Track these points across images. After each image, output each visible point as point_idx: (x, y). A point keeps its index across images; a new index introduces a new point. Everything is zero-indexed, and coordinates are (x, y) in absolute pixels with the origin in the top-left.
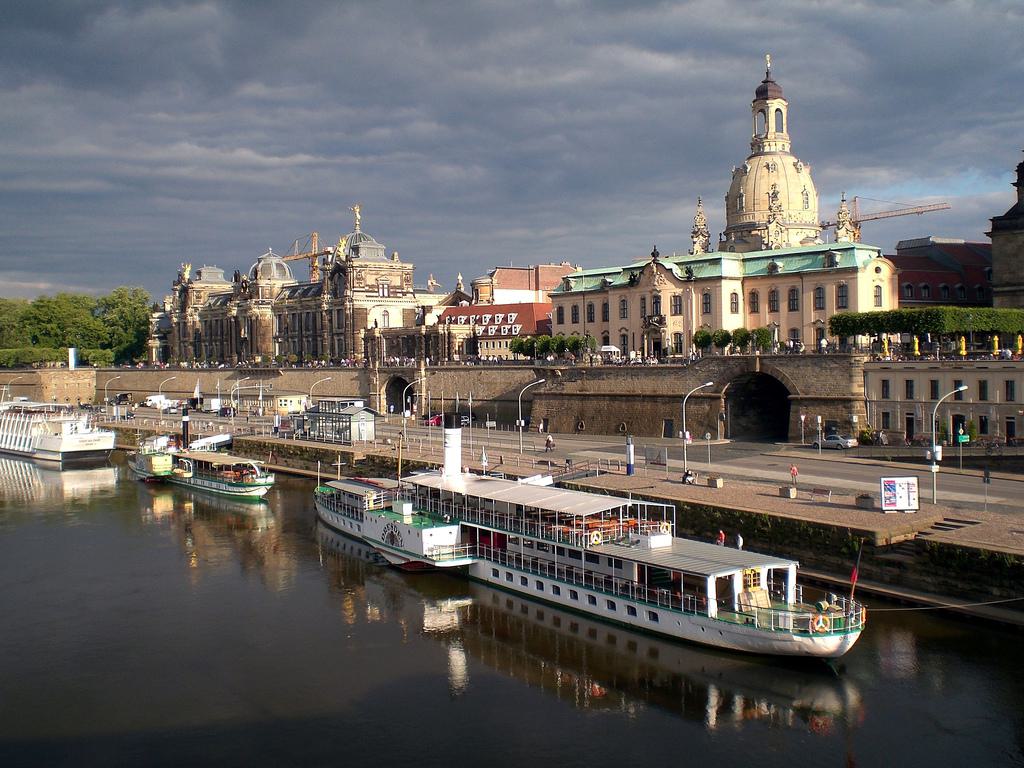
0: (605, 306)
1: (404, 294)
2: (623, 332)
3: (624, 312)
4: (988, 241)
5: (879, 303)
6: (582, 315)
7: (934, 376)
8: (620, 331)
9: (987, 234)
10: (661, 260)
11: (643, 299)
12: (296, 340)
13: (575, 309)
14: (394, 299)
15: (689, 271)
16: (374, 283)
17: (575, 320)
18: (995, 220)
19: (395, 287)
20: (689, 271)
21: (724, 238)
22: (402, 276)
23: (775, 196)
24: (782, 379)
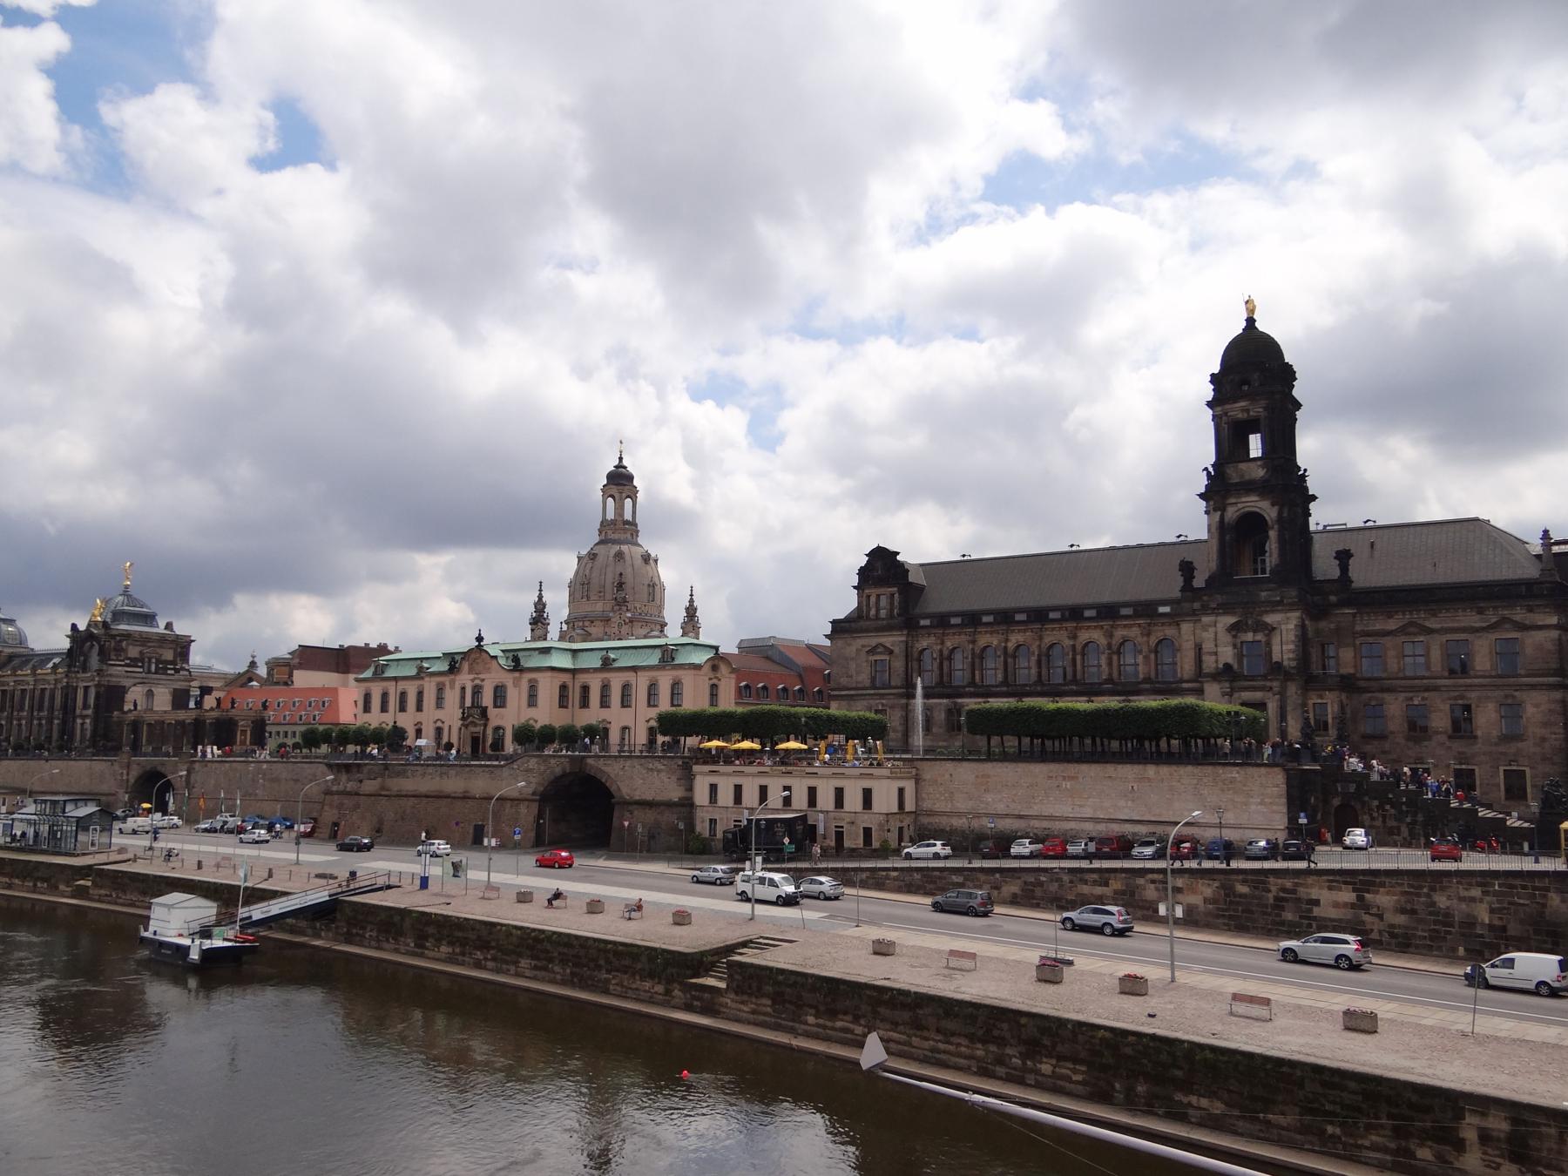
1: (177, 671)
4: (828, 643)
7: (764, 781)
11: (463, 689)
13: (385, 696)
17: (384, 709)
18: (834, 622)
20: (516, 660)
21: (565, 627)
23: (620, 586)
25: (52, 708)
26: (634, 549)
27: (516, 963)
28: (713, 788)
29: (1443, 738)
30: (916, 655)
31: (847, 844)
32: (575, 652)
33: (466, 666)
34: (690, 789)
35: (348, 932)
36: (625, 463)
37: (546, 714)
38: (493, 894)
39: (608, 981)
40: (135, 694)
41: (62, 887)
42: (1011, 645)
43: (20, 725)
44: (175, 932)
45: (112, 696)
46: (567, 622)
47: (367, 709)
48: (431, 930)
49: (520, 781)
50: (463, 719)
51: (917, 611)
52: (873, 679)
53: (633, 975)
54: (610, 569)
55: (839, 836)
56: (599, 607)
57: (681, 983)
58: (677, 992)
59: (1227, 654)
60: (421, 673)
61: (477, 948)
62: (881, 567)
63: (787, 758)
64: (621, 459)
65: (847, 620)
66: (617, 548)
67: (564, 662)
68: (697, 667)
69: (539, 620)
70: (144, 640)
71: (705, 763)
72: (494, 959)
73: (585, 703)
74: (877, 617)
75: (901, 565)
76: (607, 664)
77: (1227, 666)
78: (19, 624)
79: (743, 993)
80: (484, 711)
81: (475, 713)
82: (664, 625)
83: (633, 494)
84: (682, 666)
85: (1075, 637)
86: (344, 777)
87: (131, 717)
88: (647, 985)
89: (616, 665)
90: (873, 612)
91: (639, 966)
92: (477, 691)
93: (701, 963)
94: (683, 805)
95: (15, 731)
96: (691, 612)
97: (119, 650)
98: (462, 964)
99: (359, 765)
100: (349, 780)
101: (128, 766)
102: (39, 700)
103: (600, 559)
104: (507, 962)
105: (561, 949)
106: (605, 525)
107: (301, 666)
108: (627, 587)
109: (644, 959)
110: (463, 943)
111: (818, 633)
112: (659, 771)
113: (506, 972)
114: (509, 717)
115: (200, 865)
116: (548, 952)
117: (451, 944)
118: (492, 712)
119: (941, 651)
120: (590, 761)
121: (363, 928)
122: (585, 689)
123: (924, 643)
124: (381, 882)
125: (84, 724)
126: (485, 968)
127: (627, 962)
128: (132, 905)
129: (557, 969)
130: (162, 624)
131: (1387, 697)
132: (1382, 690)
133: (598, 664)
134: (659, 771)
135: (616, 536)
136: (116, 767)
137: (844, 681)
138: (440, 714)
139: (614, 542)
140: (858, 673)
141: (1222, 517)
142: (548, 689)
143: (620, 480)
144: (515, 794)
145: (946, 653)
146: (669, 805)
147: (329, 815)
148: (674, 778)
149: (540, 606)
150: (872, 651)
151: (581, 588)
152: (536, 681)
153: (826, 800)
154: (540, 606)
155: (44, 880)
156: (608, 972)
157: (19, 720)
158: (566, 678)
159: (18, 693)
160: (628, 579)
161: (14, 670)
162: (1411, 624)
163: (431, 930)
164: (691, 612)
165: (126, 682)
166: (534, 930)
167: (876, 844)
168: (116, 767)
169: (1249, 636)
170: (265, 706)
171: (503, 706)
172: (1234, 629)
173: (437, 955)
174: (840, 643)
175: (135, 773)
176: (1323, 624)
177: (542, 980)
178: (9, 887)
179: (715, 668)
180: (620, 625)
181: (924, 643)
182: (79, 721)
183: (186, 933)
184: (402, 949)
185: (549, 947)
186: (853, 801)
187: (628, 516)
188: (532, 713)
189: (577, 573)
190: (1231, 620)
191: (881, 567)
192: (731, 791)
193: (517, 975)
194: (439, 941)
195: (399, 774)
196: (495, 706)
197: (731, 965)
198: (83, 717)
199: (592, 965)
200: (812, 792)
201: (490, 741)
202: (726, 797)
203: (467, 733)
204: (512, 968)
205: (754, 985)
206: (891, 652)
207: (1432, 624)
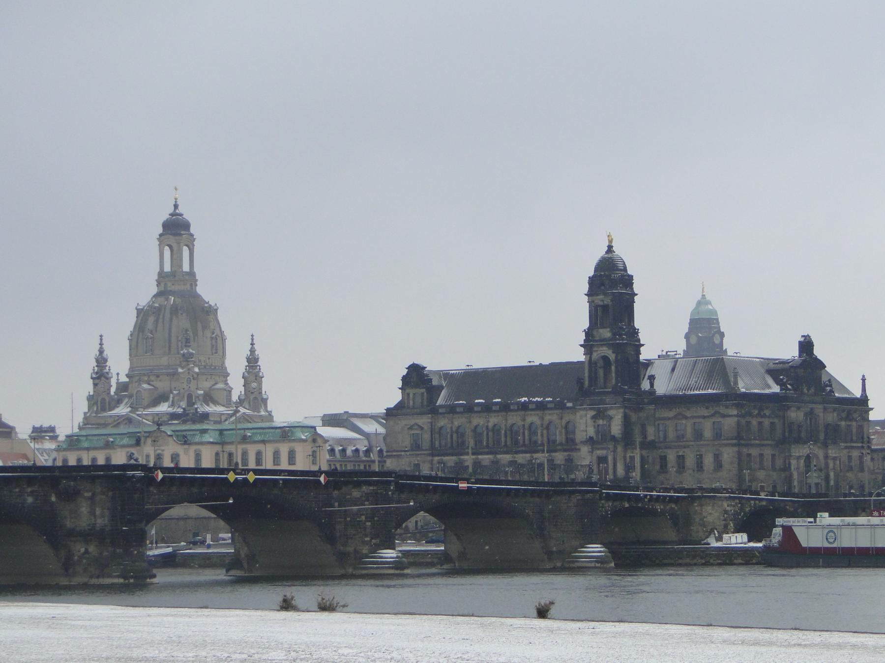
29: (691, 471)
30: (437, 430)
33: (149, 441)
36: (180, 210)
42: (491, 425)
46: (127, 376)
56: (164, 361)
59: (591, 432)
64: (176, 206)
77: (591, 438)
85: (524, 420)
90: (411, 403)
96: (253, 361)
131: (669, 451)
132: (666, 448)
141: (590, 357)
149: (101, 361)
150: (411, 428)
152: (200, 451)
154: (101, 361)
162: (679, 414)
164: (253, 361)
169: (601, 422)
172: (594, 418)
176: (641, 414)
180: (189, 381)
187: (186, 268)
190: (593, 413)
206: (422, 428)
207: (688, 414)
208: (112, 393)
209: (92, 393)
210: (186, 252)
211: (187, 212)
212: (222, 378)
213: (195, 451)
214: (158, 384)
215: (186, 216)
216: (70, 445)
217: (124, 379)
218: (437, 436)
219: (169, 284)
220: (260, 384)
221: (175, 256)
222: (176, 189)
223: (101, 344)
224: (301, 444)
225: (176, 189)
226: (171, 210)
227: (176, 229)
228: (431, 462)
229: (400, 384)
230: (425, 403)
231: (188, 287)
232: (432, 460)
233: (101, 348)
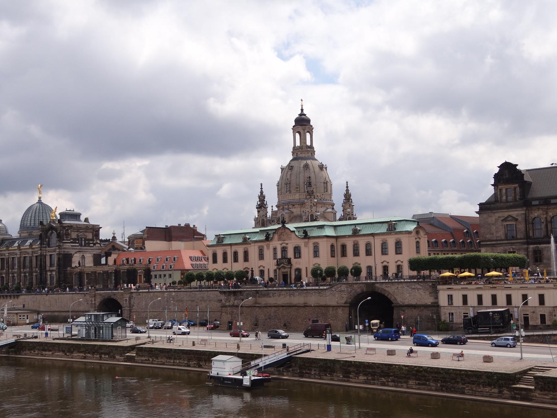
0: (246, 254)
1: (94, 244)
2: (262, 268)
3: (261, 256)
4: (478, 216)
5: (418, 251)
6: (230, 257)
7: (480, 292)
8: (259, 267)
9: (477, 212)
10: (287, 226)
11: (275, 249)
12: (27, 274)
13: (225, 255)
14: (89, 248)
15: (305, 232)
16: (76, 237)
17: (225, 260)
18: (480, 205)
19: (89, 240)
20: (305, 232)
21: (275, 209)
22: (93, 233)
23: (310, 184)
24: (388, 295)
25: (31, 267)
26: (313, 162)
27: (407, 383)
28: (450, 297)
30: (531, 221)
31: (531, 323)
32: (335, 227)
33: (276, 237)
34: (437, 298)
35: (300, 372)
36: (305, 112)
37: (325, 261)
38: (371, 352)
39: (464, 388)
40: (76, 260)
41: (117, 357)
43: (13, 277)
44: (227, 373)
45: (66, 259)
46: (277, 206)
47: (215, 261)
48: (352, 369)
49: (336, 296)
50: (278, 265)
51: (529, 196)
52: (506, 235)
53: (479, 385)
54: (302, 175)
55: (526, 319)
56: (297, 196)
57: (507, 388)
58: (505, 392)
60: (245, 241)
61: (381, 376)
62: (508, 174)
63: (490, 280)
64: (302, 110)
65: (488, 203)
66: (305, 162)
67: (330, 232)
68: (409, 232)
69: (262, 206)
70: (78, 228)
71: (444, 284)
72: (393, 381)
73: (344, 254)
74: (507, 201)
75: (519, 172)
76: (356, 233)
78: (3, 222)
79: (545, 390)
80: (289, 260)
81: (284, 261)
82: (333, 205)
83: (311, 132)
84: (401, 233)
86: (232, 298)
87: (78, 270)
88: (487, 389)
89: (361, 233)
90: (504, 198)
91: (482, 381)
92: (284, 250)
93: (515, 378)
94: (434, 306)
95: (11, 280)
96: (348, 197)
97: (68, 235)
98: (374, 384)
99: (241, 291)
100: (235, 299)
101: (95, 296)
102: (23, 264)
103: (295, 169)
104: (401, 382)
105: (434, 375)
106: (295, 149)
107: (148, 239)
108: (312, 184)
109: (484, 377)
110: (373, 374)
111: (470, 210)
112: (420, 289)
113: (402, 387)
114: (306, 263)
115: (194, 344)
116: (426, 377)
117: (365, 375)
118: (294, 261)
119: (546, 218)
120: (377, 285)
121: (311, 370)
122: (344, 247)
123: (536, 214)
124: (304, 349)
125: (52, 273)
126: (388, 386)
127: (474, 379)
128: (163, 364)
129: (432, 384)
130: (82, 218)
133: (350, 233)
134: (420, 289)
135: (303, 155)
136: (88, 297)
137: (488, 236)
138: (261, 263)
139: (302, 159)
140: (497, 232)
142: (324, 247)
143: (302, 123)
144: (334, 304)
145: (549, 219)
146: (426, 306)
147: (226, 318)
148: (428, 293)
149: (262, 198)
150: (505, 220)
151: (285, 185)
153: (517, 300)
154: (262, 198)
155: (105, 354)
156: (463, 384)
157: (13, 274)
158: (333, 241)
159: (10, 260)
160: (313, 180)
161: (7, 247)
163: (352, 369)
164: (348, 197)
165: (72, 252)
166: (416, 367)
167: (548, 323)
168: (88, 297)
170: (150, 262)
171: (300, 257)
173: (358, 381)
174: (485, 216)
175: (98, 300)
177: (424, 389)
178: (85, 358)
179: (417, 233)
180: (311, 207)
181: (536, 214)
182: (49, 273)
183: (232, 373)
184: (336, 378)
185: (426, 374)
186: (533, 300)
187: (308, 143)
188: (316, 260)
189: (282, 178)
191: (508, 174)
192: (459, 298)
193: (408, 388)
194: (357, 374)
195: (264, 295)
196: (295, 258)
197: (536, 378)
198: (51, 271)
199: (453, 381)
200: (509, 297)
201: (293, 277)
202: (458, 301)
203: (280, 274)
204: (405, 385)
205: (551, 386)
206: (516, 220)
208: (268, 216)
209: (257, 217)
210: (308, 135)
211: (308, 114)
212: (330, 206)
213: (314, 243)
214: (294, 210)
215: (308, 115)
216: (218, 242)
217: (275, 209)
218: (531, 225)
219: (299, 153)
220: (352, 209)
221: (302, 138)
222: (302, 100)
223: (261, 189)
224: (408, 235)
225: (302, 100)
226: (300, 112)
227: (302, 123)
228: (527, 250)
229: (493, 182)
230: (518, 197)
231: (310, 154)
232: (527, 248)
233: (262, 191)
